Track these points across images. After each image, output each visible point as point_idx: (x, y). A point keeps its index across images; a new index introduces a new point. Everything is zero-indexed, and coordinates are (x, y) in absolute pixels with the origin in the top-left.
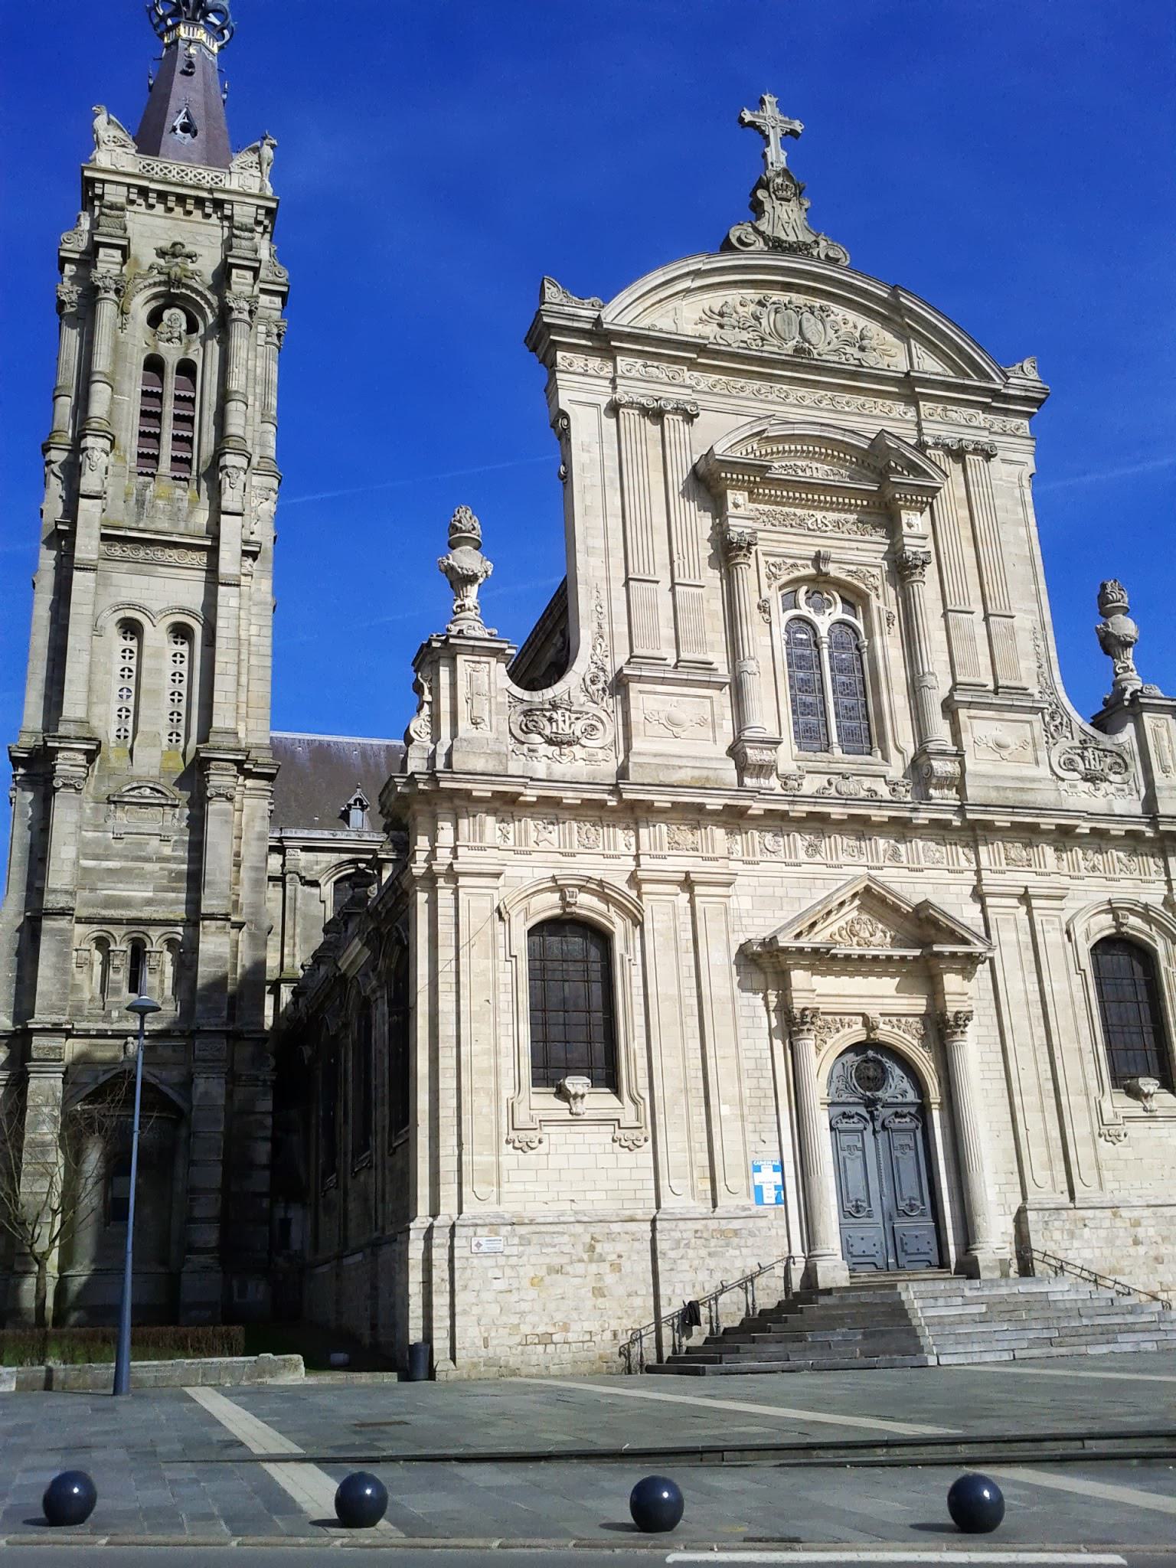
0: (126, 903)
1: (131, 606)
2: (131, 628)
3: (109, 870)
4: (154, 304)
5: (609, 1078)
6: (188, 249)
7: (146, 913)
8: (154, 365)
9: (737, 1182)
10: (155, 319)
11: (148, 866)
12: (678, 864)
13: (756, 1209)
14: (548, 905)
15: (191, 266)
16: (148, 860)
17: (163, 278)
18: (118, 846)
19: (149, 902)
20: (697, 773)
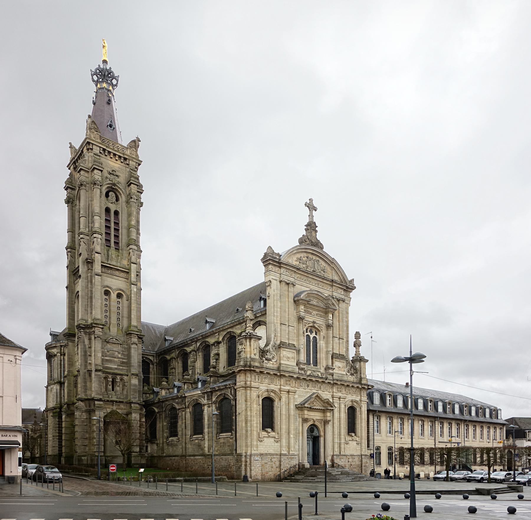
0: (111, 368)
4: (107, 190)
7: (116, 371)
8: (108, 210)
10: (107, 195)
16: (115, 358)
19: (116, 369)
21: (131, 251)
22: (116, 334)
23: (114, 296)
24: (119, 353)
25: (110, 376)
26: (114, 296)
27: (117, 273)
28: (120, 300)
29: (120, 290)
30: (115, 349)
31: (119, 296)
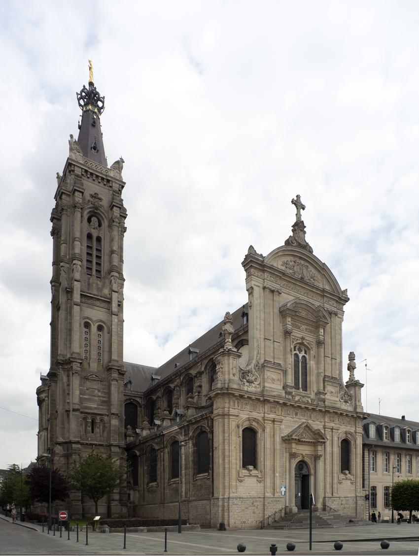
0: (90, 408)
1: (88, 318)
2: (87, 325)
3: (85, 398)
5: (255, 467)
6: (100, 196)
7: (95, 412)
8: (89, 236)
9: (278, 490)
10: (89, 220)
11: (95, 398)
12: (272, 416)
13: (281, 496)
14: (246, 424)
15: (101, 203)
16: (95, 396)
17: (92, 206)
18: (88, 392)
20: (278, 393)
21: (112, 278)
22: (96, 371)
23: (94, 328)
24: (99, 391)
25: (89, 417)
26: (94, 328)
27: (98, 303)
28: (101, 333)
29: (101, 321)
30: (94, 387)
31: (100, 328)
